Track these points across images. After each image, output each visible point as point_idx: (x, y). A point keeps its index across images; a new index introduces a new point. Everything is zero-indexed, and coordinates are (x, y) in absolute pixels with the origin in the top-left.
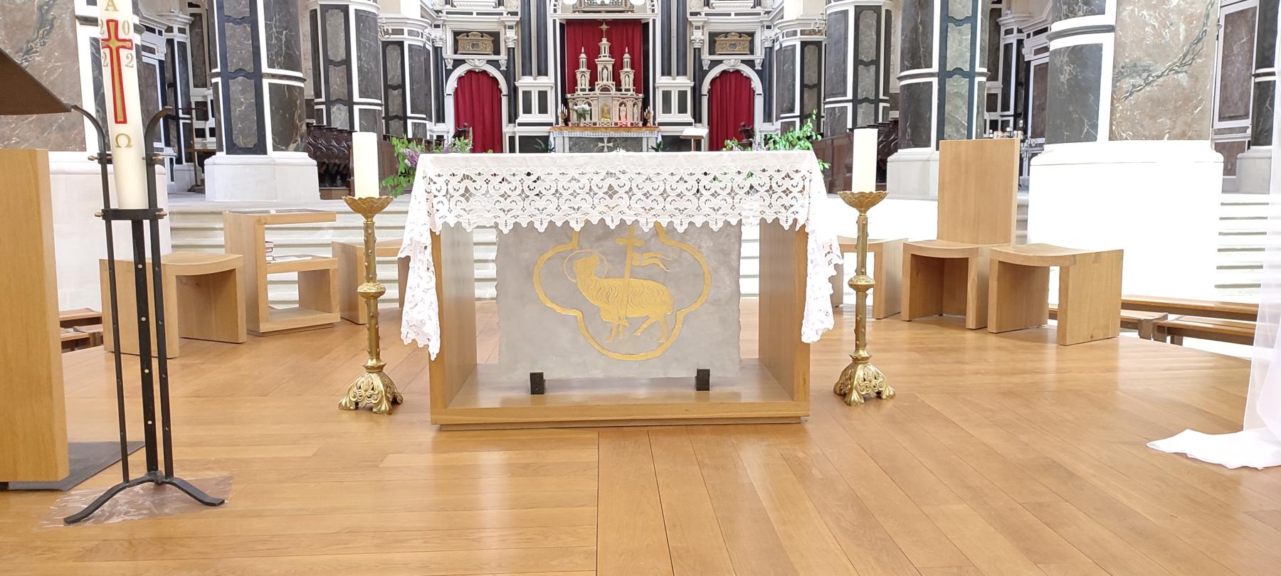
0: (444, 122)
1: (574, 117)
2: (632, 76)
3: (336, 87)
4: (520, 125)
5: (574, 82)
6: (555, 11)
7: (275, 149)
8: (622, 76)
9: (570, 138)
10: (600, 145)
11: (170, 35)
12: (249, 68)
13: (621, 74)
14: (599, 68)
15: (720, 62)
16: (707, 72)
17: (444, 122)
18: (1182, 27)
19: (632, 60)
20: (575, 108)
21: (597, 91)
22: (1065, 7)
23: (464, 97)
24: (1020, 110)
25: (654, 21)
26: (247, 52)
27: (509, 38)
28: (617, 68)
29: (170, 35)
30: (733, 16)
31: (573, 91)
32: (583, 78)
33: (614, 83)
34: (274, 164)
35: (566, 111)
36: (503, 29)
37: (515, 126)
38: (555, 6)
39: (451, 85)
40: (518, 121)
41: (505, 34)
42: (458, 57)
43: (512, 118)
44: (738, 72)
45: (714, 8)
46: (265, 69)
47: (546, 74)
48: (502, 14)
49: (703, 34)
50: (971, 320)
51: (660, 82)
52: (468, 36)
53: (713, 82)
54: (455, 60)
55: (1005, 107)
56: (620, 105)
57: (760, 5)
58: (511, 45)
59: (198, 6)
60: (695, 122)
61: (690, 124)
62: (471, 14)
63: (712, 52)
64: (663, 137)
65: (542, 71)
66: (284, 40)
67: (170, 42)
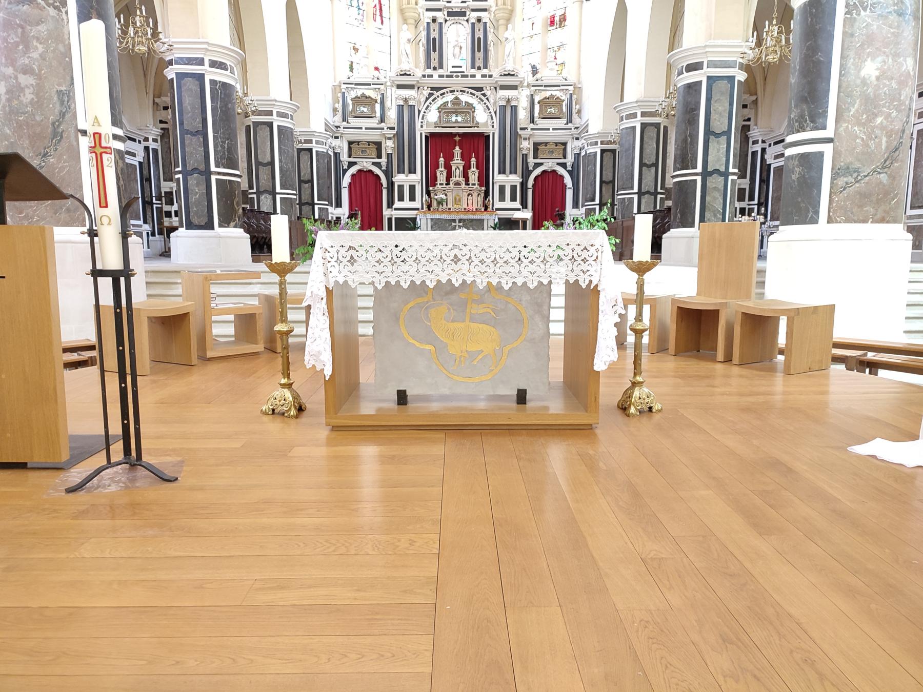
0: (341, 207)
1: (434, 204)
2: (477, 174)
3: (264, 181)
4: (396, 209)
5: (435, 179)
6: (422, 126)
7: (220, 226)
8: (470, 174)
9: (432, 219)
10: (453, 224)
11: (146, 144)
12: (202, 167)
13: (469, 173)
14: (453, 168)
15: (542, 164)
16: (532, 171)
17: (341, 207)
18: (884, 139)
19: (477, 162)
20: (436, 197)
21: (452, 185)
22: (797, 124)
23: (355, 188)
24: (762, 200)
25: (494, 134)
26: (200, 156)
27: (388, 147)
28: (467, 168)
29: (146, 144)
31: (434, 185)
32: (442, 175)
33: (464, 179)
35: (429, 200)
36: (384, 140)
37: (392, 211)
38: (422, 123)
39: (346, 181)
40: (394, 207)
41: (386, 143)
42: (352, 160)
43: (390, 205)
44: (554, 172)
45: (537, 125)
46: (213, 168)
47: (415, 173)
48: (383, 129)
49: (529, 144)
50: (720, 356)
51: (498, 178)
52: (359, 145)
53: (536, 178)
54: (349, 162)
55: (751, 198)
56: (468, 195)
57: (571, 122)
58: (390, 151)
59: (166, 123)
60: (523, 208)
61: (519, 210)
62: (361, 128)
63: (535, 157)
64: (499, 219)
65: (412, 171)
66: (226, 147)
67: (147, 149)
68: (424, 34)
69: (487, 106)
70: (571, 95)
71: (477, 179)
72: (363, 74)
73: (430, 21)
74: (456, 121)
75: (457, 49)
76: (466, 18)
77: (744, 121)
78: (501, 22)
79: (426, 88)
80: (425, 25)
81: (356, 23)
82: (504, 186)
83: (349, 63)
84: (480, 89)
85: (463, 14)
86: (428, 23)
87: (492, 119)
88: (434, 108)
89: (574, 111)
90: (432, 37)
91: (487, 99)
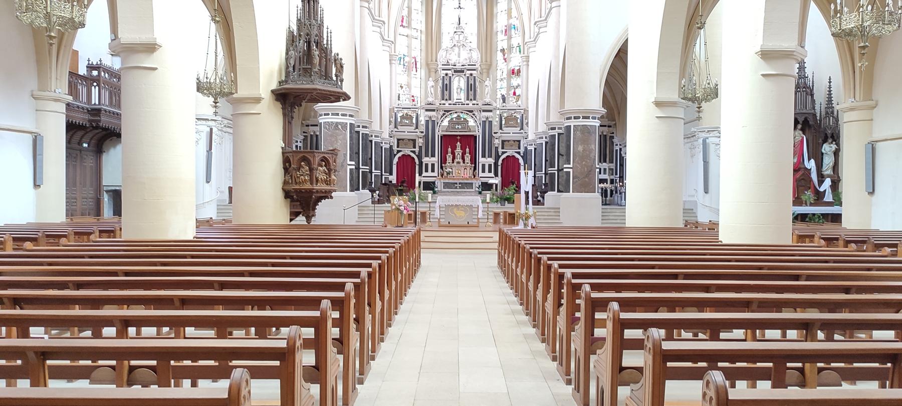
1: (445, 174)
2: (469, 158)
4: (423, 177)
5: (446, 160)
6: (439, 131)
7: (362, 189)
8: (465, 157)
9: (444, 183)
10: (456, 185)
11: (296, 144)
14: (456, 154)
15: (506, 152)
18: (586, 168)
19: (470, 151)
20: (446, 170)
21: (455, 164)
23: (400, 164)
24: (621, 175)
28: (464, 154)
29: (296, 144)
30: (511, 134)
34: (362, 194)
35: (442, 172)
39: (396, 160)
40: (423, 175)
43: (420, 174)
44: (514, 156)
46: (361, 167)
47: (434, 157)
50: (516, 223)
55: (616, 174)
58: (420, 145)
59: (306, 133)
60: (495, 176)
61: (493, 177)
62: (405, 132)
63: (503, 148)
64: (482, 182)
65: (433, 156)
68: (440, 82)
69: (476, 121)
70: (522, 115)
71: (469, 160)
72: (405, 102)
73: (444, 75)
74: (458, 128)
75: (459, 90)
76: (464, 74)
77: (611, 133)
78: (484, 71)
79: (441, 111)
80: (442, 77)
81: (402, 73)
82: (485, 164)
83: (397, 95)
84: (471, 111)
85: (463, 72)
86: (443, 77)
87: (478, 127)
88: (448, 119)
89: (524, 123)
90: (445, 83)
91: (476, 117)
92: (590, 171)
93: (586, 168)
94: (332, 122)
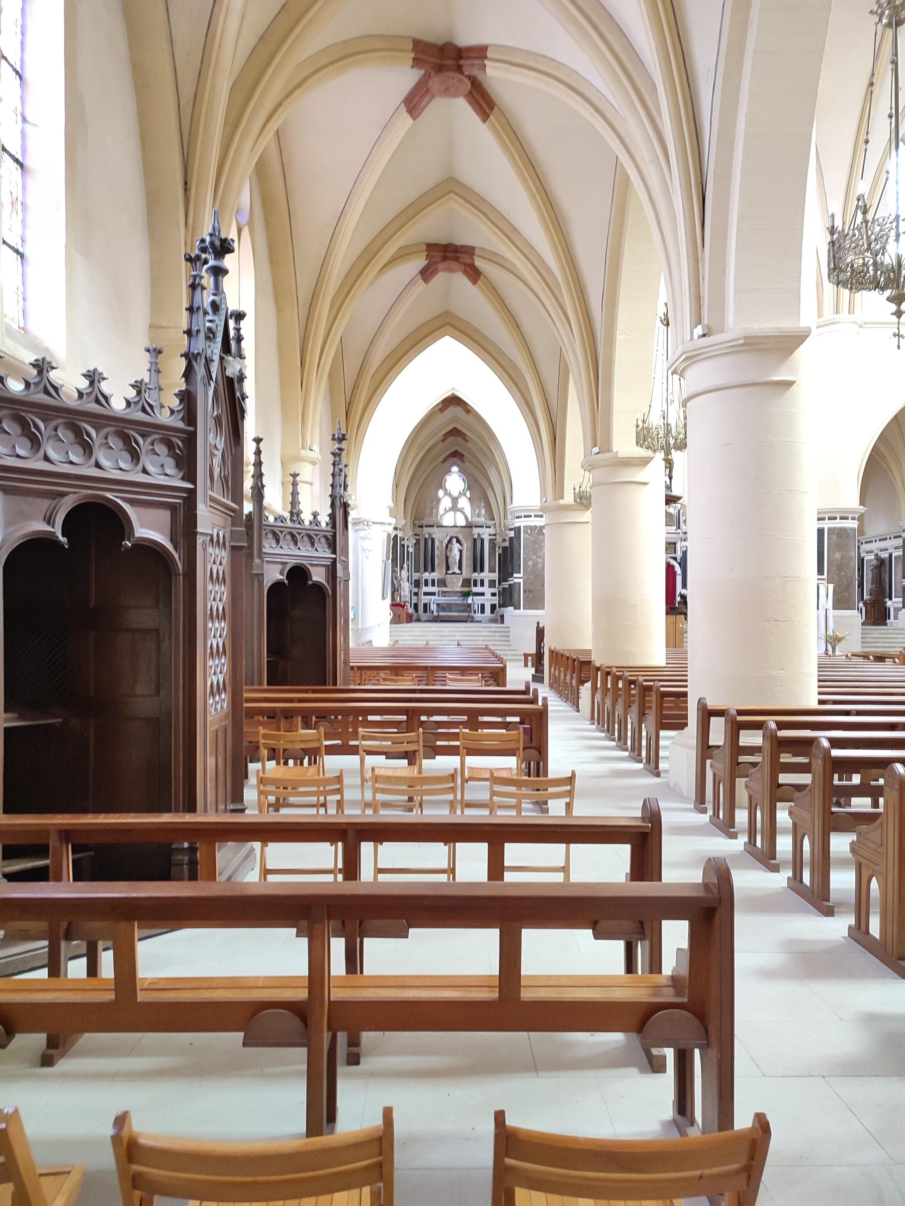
18: (845, 581)
70: (679, 511)
92: (850, 583)
93: (845, 581)
94: (535, 526)
